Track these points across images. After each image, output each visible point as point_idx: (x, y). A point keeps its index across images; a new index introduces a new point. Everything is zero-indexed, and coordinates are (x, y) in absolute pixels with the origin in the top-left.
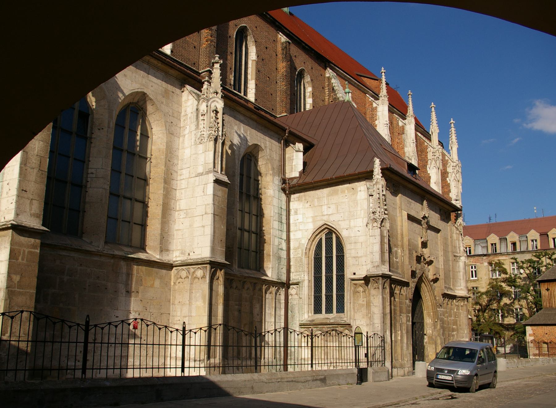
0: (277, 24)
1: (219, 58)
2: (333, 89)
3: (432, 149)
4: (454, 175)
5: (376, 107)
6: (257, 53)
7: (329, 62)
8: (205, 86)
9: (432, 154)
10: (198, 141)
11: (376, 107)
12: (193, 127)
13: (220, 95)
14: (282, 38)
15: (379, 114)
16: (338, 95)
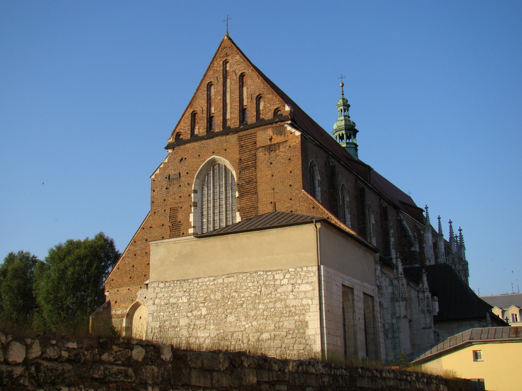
0: (380, 194)
1: (425, 271)
2: (403, 228)
3: (452, 256)
4: (463, 272)
5: (423, 234)
6: (375, 218)
7: (400, 209)
8: (421, 285)
9: (452, 259)
10: (421, 312)
11: (423, 234)
12: (417, 304)
13: (428, 290)
14: (383, 204)
15: (426, 239)
16: (407, 233)
